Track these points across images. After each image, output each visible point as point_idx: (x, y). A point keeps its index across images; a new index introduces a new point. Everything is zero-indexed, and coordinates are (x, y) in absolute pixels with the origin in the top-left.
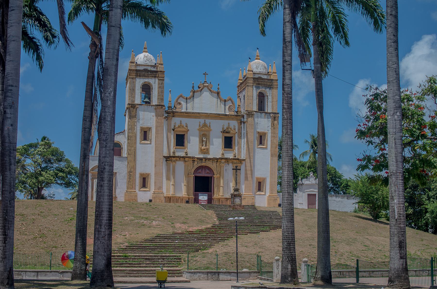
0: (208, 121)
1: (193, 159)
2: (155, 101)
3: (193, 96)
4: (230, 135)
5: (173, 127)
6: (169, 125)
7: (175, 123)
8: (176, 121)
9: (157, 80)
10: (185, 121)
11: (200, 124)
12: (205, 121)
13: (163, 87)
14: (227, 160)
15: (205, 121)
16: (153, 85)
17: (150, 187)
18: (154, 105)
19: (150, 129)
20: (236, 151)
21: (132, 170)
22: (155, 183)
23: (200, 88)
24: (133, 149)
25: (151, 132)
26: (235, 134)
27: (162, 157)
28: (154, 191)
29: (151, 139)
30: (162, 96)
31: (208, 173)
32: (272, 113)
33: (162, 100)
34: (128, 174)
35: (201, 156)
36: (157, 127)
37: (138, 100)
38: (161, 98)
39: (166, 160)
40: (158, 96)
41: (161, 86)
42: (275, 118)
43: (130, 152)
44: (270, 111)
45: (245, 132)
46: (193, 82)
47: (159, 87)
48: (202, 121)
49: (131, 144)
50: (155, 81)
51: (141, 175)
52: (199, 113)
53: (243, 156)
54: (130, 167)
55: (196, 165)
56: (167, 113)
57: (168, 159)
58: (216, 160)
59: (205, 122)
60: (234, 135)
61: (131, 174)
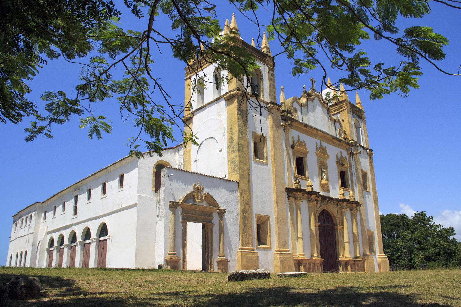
0: (324, 144)
2: (266, 96)
3: (307, 105)
4: (344, 168)
5: (291, 143)
6: (287, 139)
7: (293, 138)
8: (294, 134)
9: (266, 68)
10: (304, 137)
11: (317, 147)
12: (321, 143)
13: (274, 80)
15: (321, 143)
16: (263, 72)
17: (271, 244)
21: (247, 207)
22: (279, 234)
23: (312, 96)
24: (246, 168)
25: (267, 146)
26: (347, 168)
27: (284, 190)
29: (267, 157)
30: (274, 93)
32: (369, 149)
33: (275, 98)
34: (242, 215)
36: (274, 137)
38: (273, 95)
39: (289, 196)
40: (270, 90)
41: (271, 77)
42: (370, 155)
43: (242, 174)
45: (354, 167)
46: (304, 86)
47: (270, 79)
49: (243, 159)
50: (264, 68)
51: (259, 218)
52: (317, 130)
53: (357, 200)
54: (243, 202)
55: (320, 207)
57: (290, 195)
59: (321, 145)
60: (346, 169)
61: (246, 215)
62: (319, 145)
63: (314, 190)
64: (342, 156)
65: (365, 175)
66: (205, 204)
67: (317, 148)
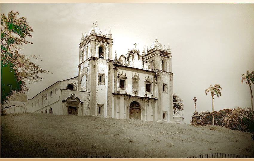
0: (137, 74)
1: (130, 96)
2: (107, 57)
14: (149, 99)
17: (104, 114)
18: (107, 60)
19: (103, 75)
20: (153, 94)
28: (107, 116)
31: (137, 107)
35: (134, 95)
37: (97, 55)
44: (168, 71)
48: (134, 73)
56: (114, 65)
58: (142, 98)
62: (134, 74)
63: (128, 94)
64: (148, 78)
65: (164, 85)
66: (76, 100)
67: (133, 76)
